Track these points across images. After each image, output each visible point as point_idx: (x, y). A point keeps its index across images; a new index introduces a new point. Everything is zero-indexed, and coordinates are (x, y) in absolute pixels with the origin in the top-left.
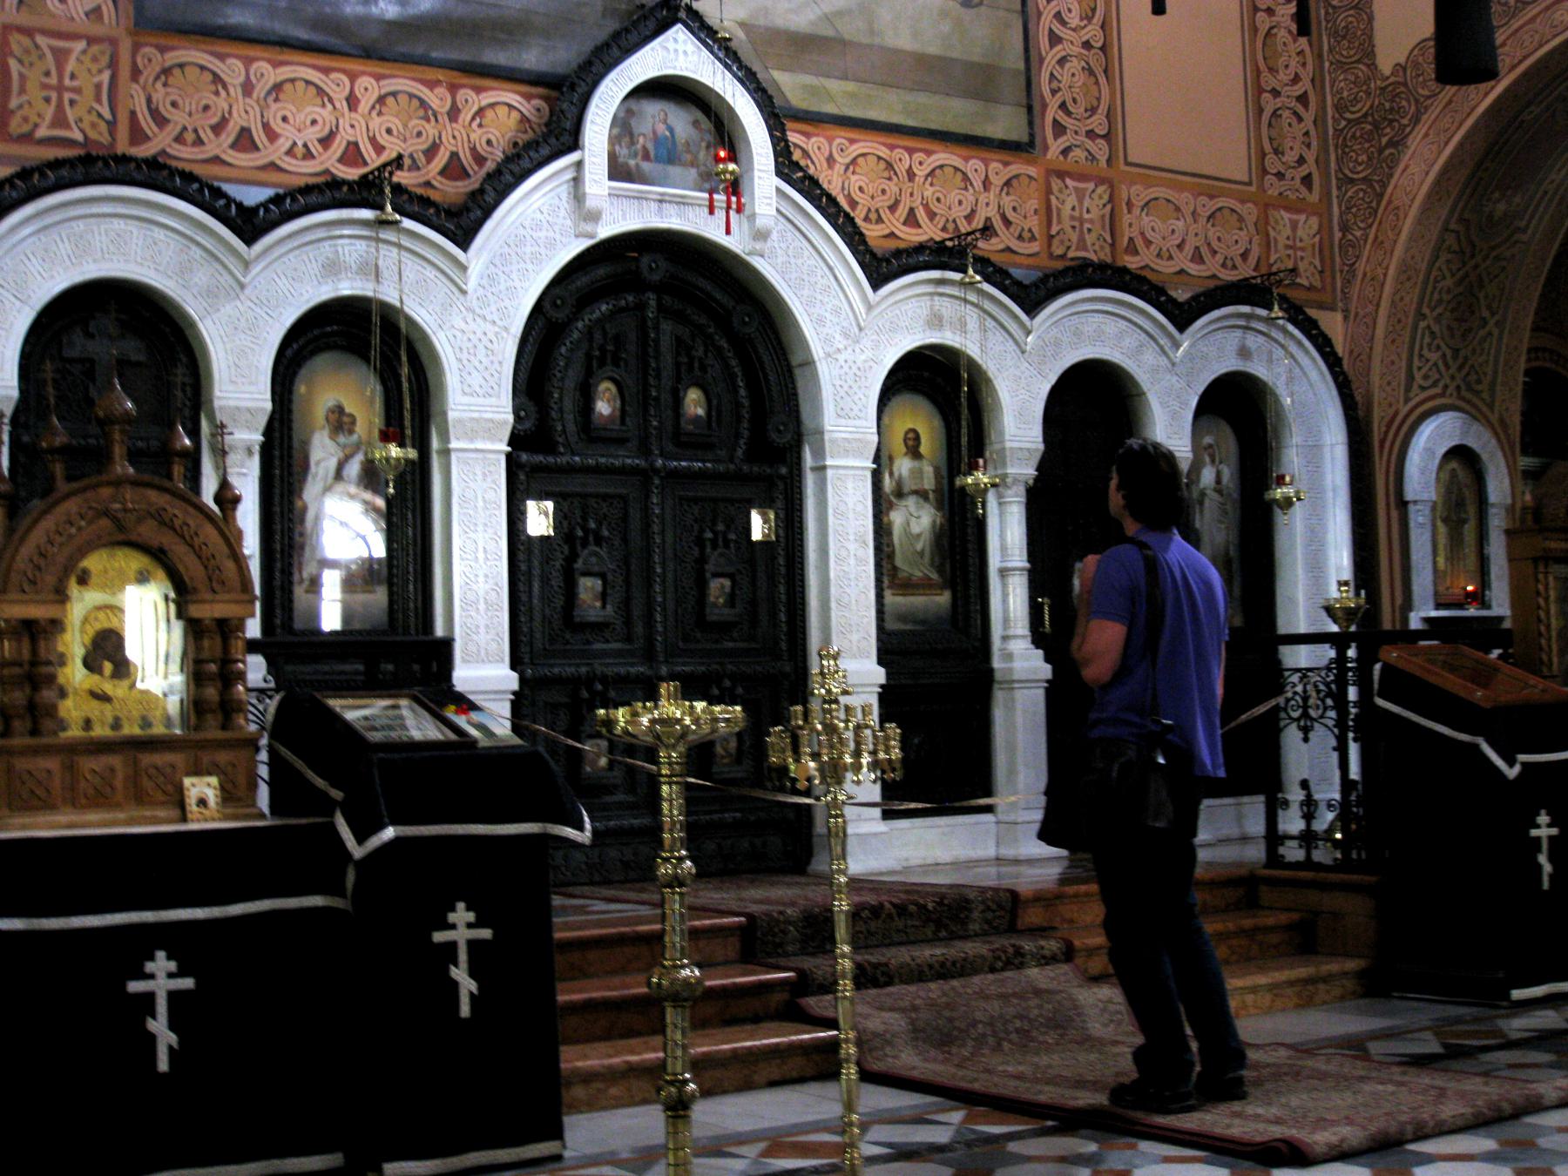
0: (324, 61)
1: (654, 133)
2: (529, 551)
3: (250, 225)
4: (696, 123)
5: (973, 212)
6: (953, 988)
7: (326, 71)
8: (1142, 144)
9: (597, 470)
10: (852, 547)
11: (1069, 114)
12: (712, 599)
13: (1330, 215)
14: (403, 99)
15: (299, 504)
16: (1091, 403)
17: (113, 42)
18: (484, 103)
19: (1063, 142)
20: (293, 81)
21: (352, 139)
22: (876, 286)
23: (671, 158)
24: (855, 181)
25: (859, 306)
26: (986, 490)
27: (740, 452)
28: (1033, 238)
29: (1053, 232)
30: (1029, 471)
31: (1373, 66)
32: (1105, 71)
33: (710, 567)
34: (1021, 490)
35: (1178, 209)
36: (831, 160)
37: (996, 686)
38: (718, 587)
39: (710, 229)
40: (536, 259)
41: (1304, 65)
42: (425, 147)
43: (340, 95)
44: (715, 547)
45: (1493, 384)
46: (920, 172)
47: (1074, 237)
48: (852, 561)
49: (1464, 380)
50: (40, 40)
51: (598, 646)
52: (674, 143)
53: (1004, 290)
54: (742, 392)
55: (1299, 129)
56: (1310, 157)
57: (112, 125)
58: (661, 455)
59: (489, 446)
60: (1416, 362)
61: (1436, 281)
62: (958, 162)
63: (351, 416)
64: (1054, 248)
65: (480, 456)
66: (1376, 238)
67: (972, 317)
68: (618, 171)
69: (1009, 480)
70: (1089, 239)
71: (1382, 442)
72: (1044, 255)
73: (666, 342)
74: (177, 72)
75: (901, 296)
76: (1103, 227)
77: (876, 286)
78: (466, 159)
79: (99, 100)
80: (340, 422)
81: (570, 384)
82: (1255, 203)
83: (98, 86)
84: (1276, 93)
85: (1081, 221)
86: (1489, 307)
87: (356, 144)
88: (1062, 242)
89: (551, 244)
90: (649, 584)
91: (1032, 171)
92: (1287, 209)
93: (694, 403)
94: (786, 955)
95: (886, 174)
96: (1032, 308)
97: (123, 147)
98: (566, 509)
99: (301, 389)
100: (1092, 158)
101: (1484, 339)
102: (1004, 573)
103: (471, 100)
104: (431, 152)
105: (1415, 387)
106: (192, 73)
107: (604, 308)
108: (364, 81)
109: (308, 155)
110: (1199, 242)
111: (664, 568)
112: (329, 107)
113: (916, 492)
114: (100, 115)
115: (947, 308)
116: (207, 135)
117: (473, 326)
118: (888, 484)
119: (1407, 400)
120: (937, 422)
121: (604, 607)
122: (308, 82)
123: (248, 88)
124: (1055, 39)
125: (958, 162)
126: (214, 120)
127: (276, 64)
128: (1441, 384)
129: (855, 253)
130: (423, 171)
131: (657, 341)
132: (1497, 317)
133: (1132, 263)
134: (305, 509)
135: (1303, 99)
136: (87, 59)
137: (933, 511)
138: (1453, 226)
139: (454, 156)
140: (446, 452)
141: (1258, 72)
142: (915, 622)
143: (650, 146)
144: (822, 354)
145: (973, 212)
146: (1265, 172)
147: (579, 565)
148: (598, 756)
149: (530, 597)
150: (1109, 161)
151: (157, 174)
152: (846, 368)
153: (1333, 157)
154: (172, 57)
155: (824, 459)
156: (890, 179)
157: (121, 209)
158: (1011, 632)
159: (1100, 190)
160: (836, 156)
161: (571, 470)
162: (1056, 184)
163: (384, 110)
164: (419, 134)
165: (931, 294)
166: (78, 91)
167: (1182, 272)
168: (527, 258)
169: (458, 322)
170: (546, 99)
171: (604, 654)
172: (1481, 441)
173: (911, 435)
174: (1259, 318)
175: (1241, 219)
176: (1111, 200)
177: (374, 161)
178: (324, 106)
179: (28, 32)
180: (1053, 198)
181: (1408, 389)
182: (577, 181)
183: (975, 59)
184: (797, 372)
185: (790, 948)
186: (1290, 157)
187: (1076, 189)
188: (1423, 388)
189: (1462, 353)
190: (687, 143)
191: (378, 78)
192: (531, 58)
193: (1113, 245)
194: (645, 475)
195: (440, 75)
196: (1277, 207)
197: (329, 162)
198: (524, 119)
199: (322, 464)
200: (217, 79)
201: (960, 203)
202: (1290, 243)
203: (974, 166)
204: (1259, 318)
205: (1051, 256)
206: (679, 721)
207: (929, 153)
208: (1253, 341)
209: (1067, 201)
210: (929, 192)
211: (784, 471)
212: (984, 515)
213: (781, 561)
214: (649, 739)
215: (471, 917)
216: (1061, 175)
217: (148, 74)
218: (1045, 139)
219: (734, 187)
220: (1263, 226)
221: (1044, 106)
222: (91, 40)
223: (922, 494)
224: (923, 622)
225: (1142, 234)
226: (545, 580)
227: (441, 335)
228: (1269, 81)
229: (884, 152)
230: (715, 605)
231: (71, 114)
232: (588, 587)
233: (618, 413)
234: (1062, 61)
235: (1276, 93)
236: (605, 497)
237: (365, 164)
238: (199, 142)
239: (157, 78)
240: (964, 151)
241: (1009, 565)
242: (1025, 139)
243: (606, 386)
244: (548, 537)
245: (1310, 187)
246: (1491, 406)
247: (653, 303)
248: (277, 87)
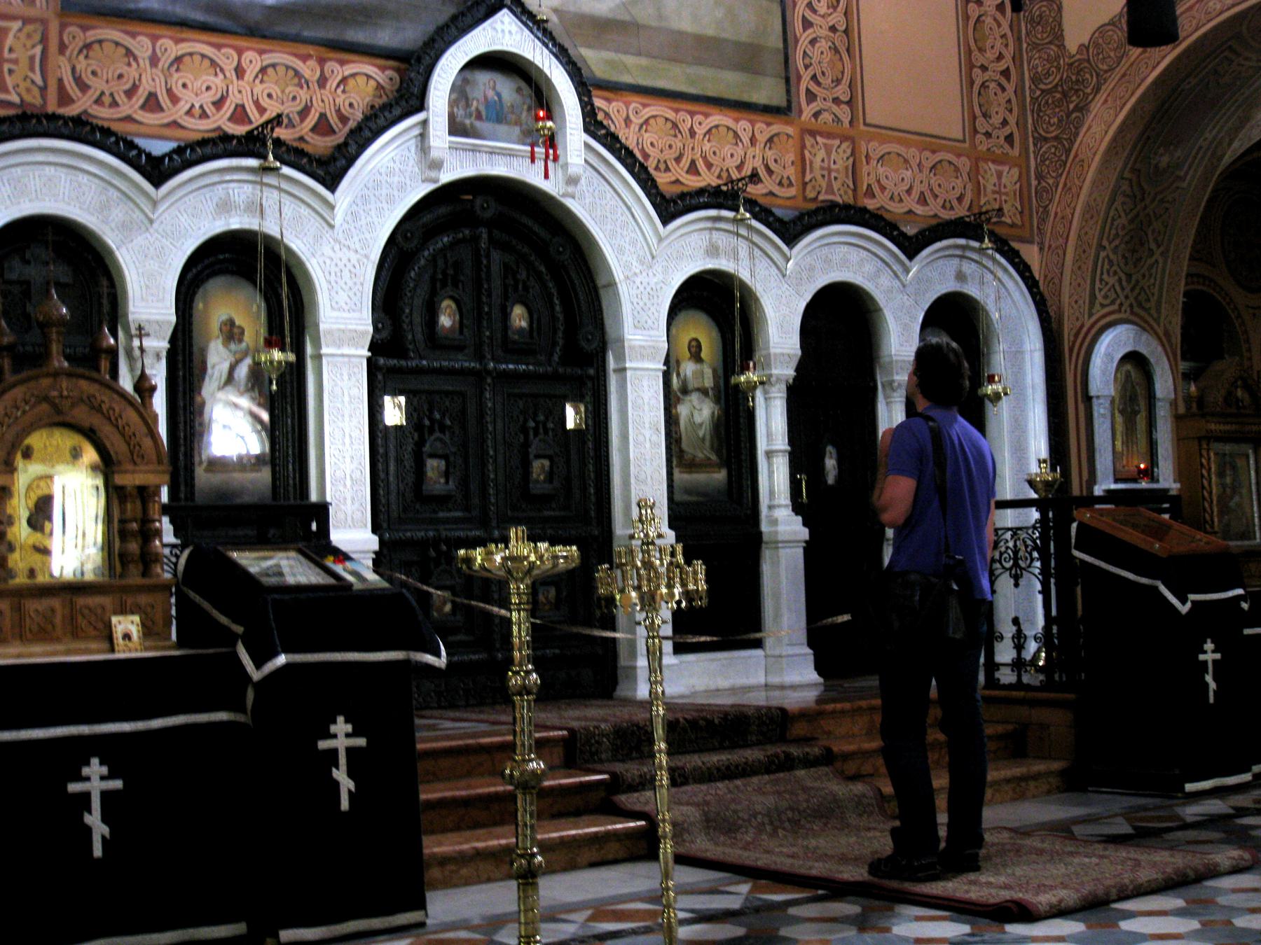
0: (215, 39)
1: (486, 97)
2: (386, 438)
3: (157, 171)
4: (519, 90)
5: (742, 163)
6: (737, 787)
7: (218, 47)
8: (877, 109)
9: (440, 372)
10: (648, 433)
11: (819, 84)
12: (535, 476)
13: (1028, 167)
14: (281, 70)
15: (198, 399)
16: (840, 318)
17: (44, 22)
18: (346, 73)
19: (815, 107)
20: (191, 54)
21: (240, 102)
22: (665, 222)
23: (500, 119)
24: (648, 137)
25: (653, 240)
26: (755, 388)
27: (556, 358)
28: (790, 184)
29: (807, 179)
30: (790, 372)
31: (1062, 46)
32: (848, 50)
33: (532, 451)
34: (784, 387)
35: (906, 161)
36: (628, 121)
37: (764, 546)
38: (539, 467)
39: (532, 175)
40: (391, 200)
41: (1006, 45)
42: (299, 108)
43: (229, 67)
44: (536, 435)
45: (1159, 303)
46: (700, 131)
47: (824, 185)
48: (648, 445)
49: (1136, 299)
51: (441, 514)
53: (769, 226)
54: (558, 308)
55: (1003, 98)
56: (1012, 120)
57: (43, 90)
58: (493, 359)
59: (352, 351)
60: (1098, 285)
61: (1113, 220)
62: (730, 123)
63: (240, 327)
64: (808, 192)
65: (346, 359)
66: (1065, 184)
67: (743, 247)
68: (456, 128)
69: (773, 379)
70: (836, 185)
71: (1071, 350)
72: (800, 198)
73: (495, 268)
74: (96, 46)
75: (682, 231)
76: (847, 177)
77: (665, 222)
78: (333, 120)
79: (32, 69)
80: (231, 333)
81: (418, 302)
82: (968, 157)
83: (32, 58)
84: (984, 68)
86: (1155, 240)
87: (243, 106)
88: (814, 187)
89: (402, 188)
90: (483, 465)
91: (790, 130)
92: (994, 162)
93: (519, 317)
94: (601, 761)
95: (672, 132)
96: (791, 240)
97: (52, 108)
98: (415, 403)
99: (199, 305)
100: (837, 120)
101: (1151, 266)
102: (769, 454)
103: (336, 70)
104: (304, 113)
105: (1097, 306)
106: (108, 47)
107: (445, 239)
108: (249, 55)
109: (204, 115)
110: (924, 187)
111: (495, 451)
112: (221, 76)
113: (698, 390)
114: (33, 82)
115: (722, 239)
116: (121, 98)
117: (339, 254)
118: (675, 381)
119: (1091, 315)
120: (715, 334)
121: (447, 482)
122: (203, 56)
123: (154, 61)
124: (807, 24)
125: (730, 123)
126: (127, 86)
128: (1118, 302)
129: (648, 195)
130: (297, 129)
131: (488, 267)
132: (1162, 249)
133: (871, 204)
134: (203, 404)
135: (1006, 73)
136: (22, 36)
137: (712, 405)
138: (1127, 175)
139: (323, 116)
140: (318, 357)
141: (970, 52)
142: (698, 494)
143: (482, 108)
144: (622, 277)
145: (742, 163)
146: (976, 131)
147: (427, 448)
148: (444, 603)
149: (387, 474)
150: (851, 122)
151: (82, 130)
152: (641, 288)
153: (1030, 121)
154: (92, 35)
155: (624, 361)
156: (675, 136)
157: (52, 158)
158: (776, 502)
159: (845, 145)
160: (632, 117)
161: (419, 371)
162: (809, 141)
163: (265, 78)
164: (294, 98)
165: (711, 229)
166: (16, 62)
167: (910, 212)
168: (383, 198)
169: (327, 250)
170: (398, 70)
171: (447, 521)
172: (1150, 348)
173: (694, 343)
174: (973, 249)
175: (957, 169)
176: (853, 153)
177: (257, 119)
178: (216, 74)
180: (806, 152)
181: (1092, 304)
182: (423, 136)
183: (744, 39)
184: (602, 292)
185: (603, 756)
186: (996, 120)
187: (825, 145)
188: (1103, 306)
189: (1134, 278)
190: (512, 106)
191: (261, 52)
192: (385, 37)
193: (855, 190)
194: (478, 376)
195: (311, 50)
196: (986, 160)
197: (221, 121)
198: (379, 87)
199: (217, 368)
200: (129, 53)
201: (732, 155)
202: (996, 189)
203: (743, 126)
204: (973, 249)
205: (805, 198)
206: (526, 558)
207: (706, 115)
208: (968, 268)
209: (817, 156)
210: (707, 147)
211: (591, 372)
212: (754, 408)
213: (590, 445)
214: (502, 573)
215: (349, 728)
216: (813, 133)
217: (73, 48)
218: (799, 103)
219: (551, 142)
220: (975, 174)
221: (799, 78)
222: (26, 21)
223: (704, 392)
224: (705, 494)
225: (879, 181)
226: (399, 461)
227: (314, 261)
228: (979, 59)
229: (671, 115)
230: (537, 481)
232: (433, 466)
233: (457, 325)
234: (813, 42)
235: (984, 68)
236: (447, 393)
237: (250, 122)
238: (114, 104)
239: (80, 51)
240: (736, 114)
241: (775, 448)
242: (784, 104)
243: (446, 303)
244: (402, 426)
245: (1012, 146)
246: (1157, 321)
247: (485, 236)
248: (178, 60)
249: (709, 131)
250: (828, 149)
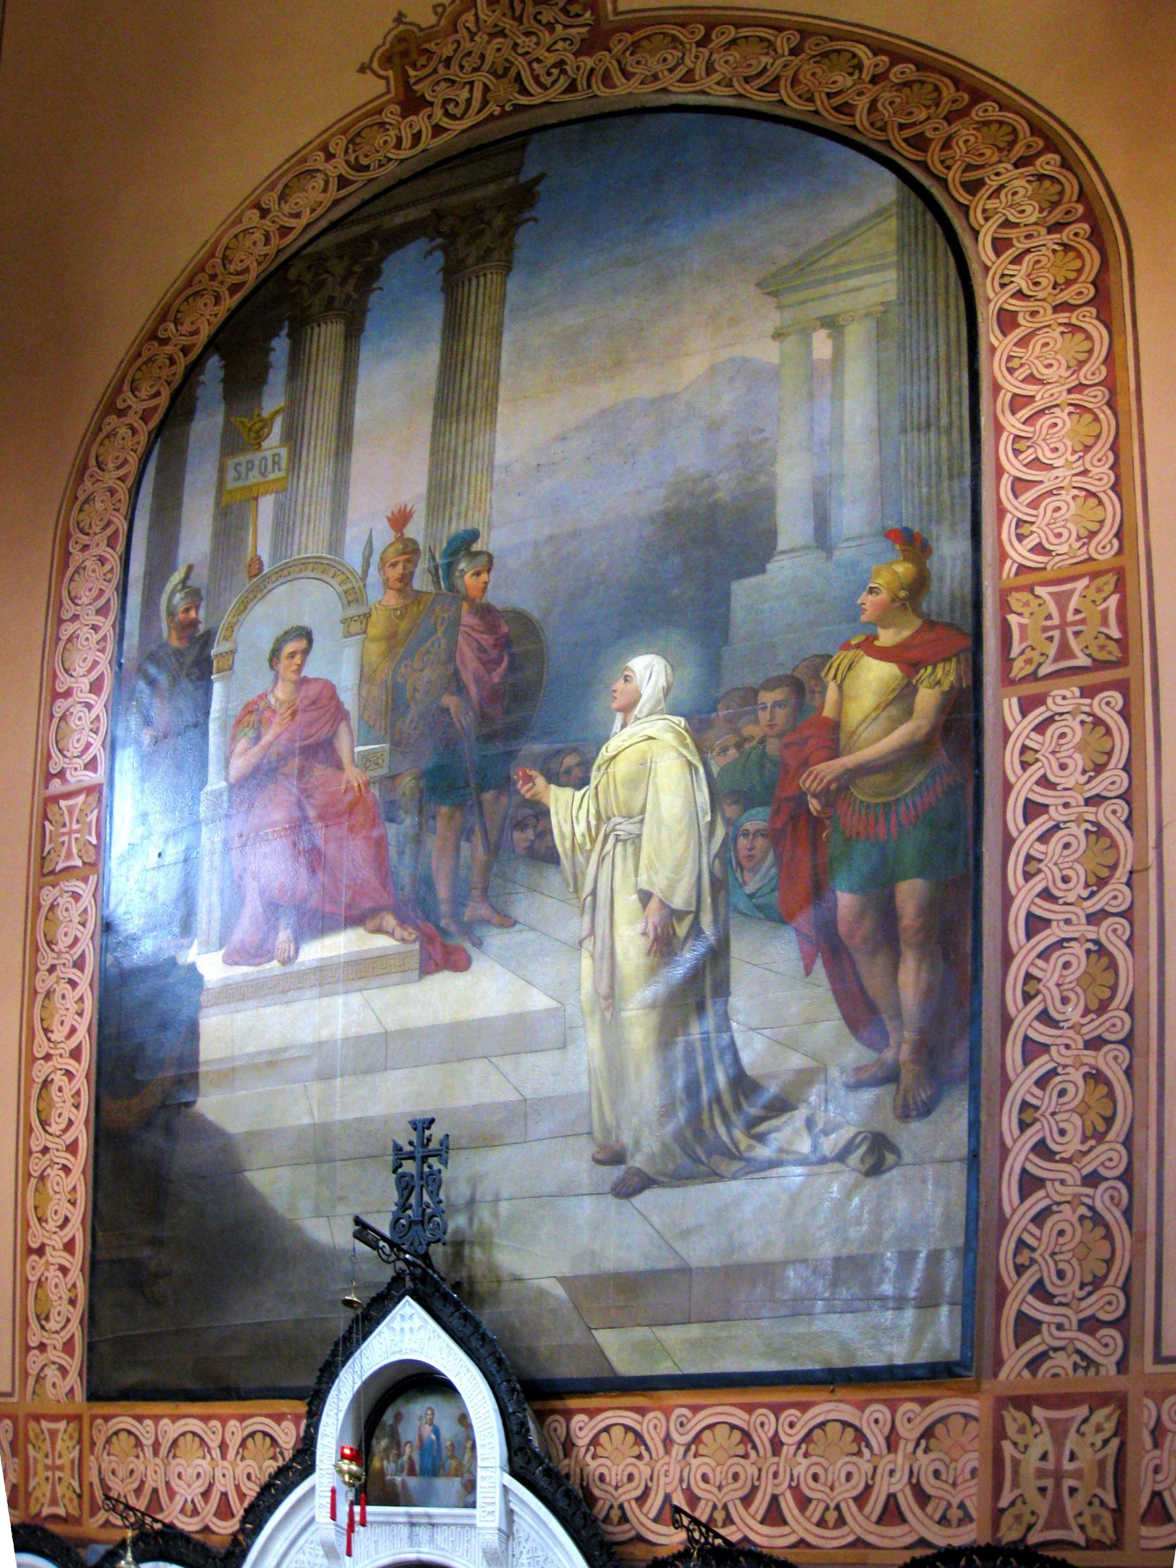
5: (868, 1488)
46: (790, 1439)
52: (439, 1450)
85: (1058, 1476)
91: (971, 1405)
150: (1122, 1365)
156: (746, 1456)
159: (1100, 1415)
162: (1013, 1419)
176: (1121, 1429)
180: (1007, 1446)
187: (1051, 1422)
201: (849, 1476)
203: (874, 1417)
209: (1032, 1448)
210: (802, 1467)
229: (739, 1418)
240: (860, 1395)
249: (807, 1438)
250: (1059, 1431)
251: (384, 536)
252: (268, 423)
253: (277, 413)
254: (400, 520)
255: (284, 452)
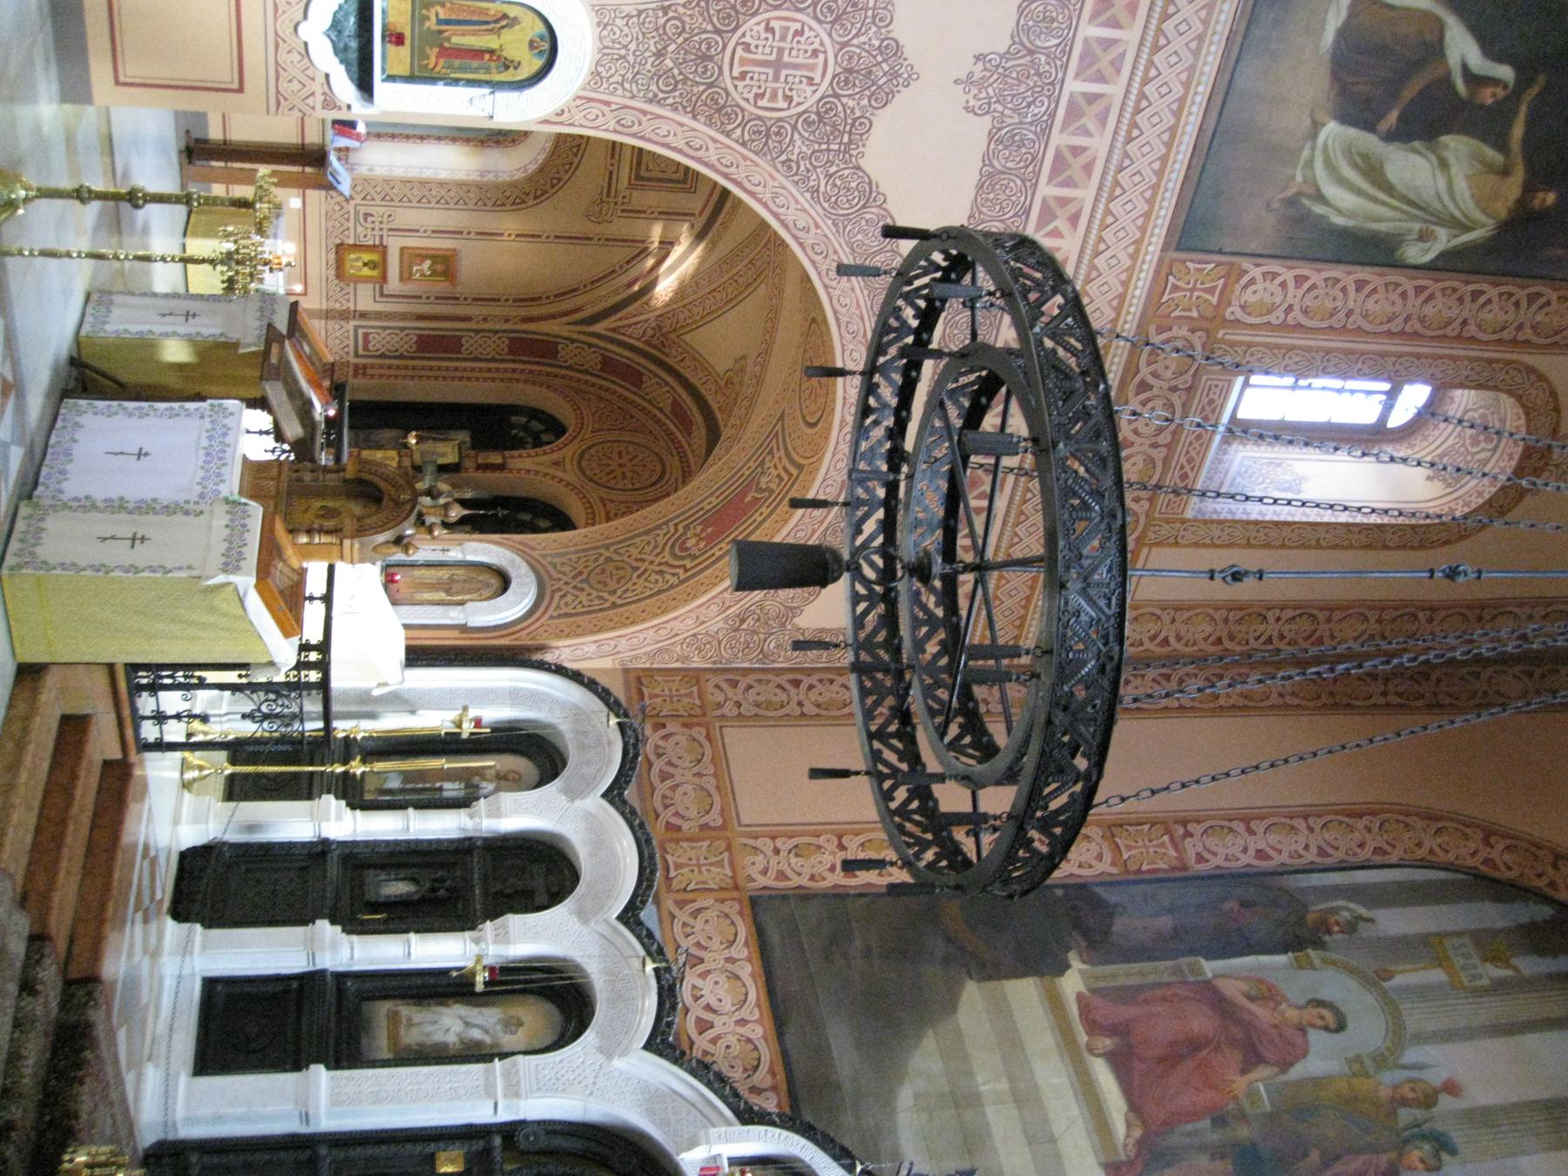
7: (758, 1005)
14: (755, 1054)
43: (744, 1014)
50: (726, 855)
87: (712, 1027)
99: (532, 999)
109: (696, 999)
127: (752, 975)
166: (700, 872)
179: (728, 848)
195: (781, 1077)
231: (685, 870)
248: (737, 977)
251: (1435, 1077)
252: (1508, 966)
253: (1516, 969)
254: (1451, 1088)
255: (1485, 982)
